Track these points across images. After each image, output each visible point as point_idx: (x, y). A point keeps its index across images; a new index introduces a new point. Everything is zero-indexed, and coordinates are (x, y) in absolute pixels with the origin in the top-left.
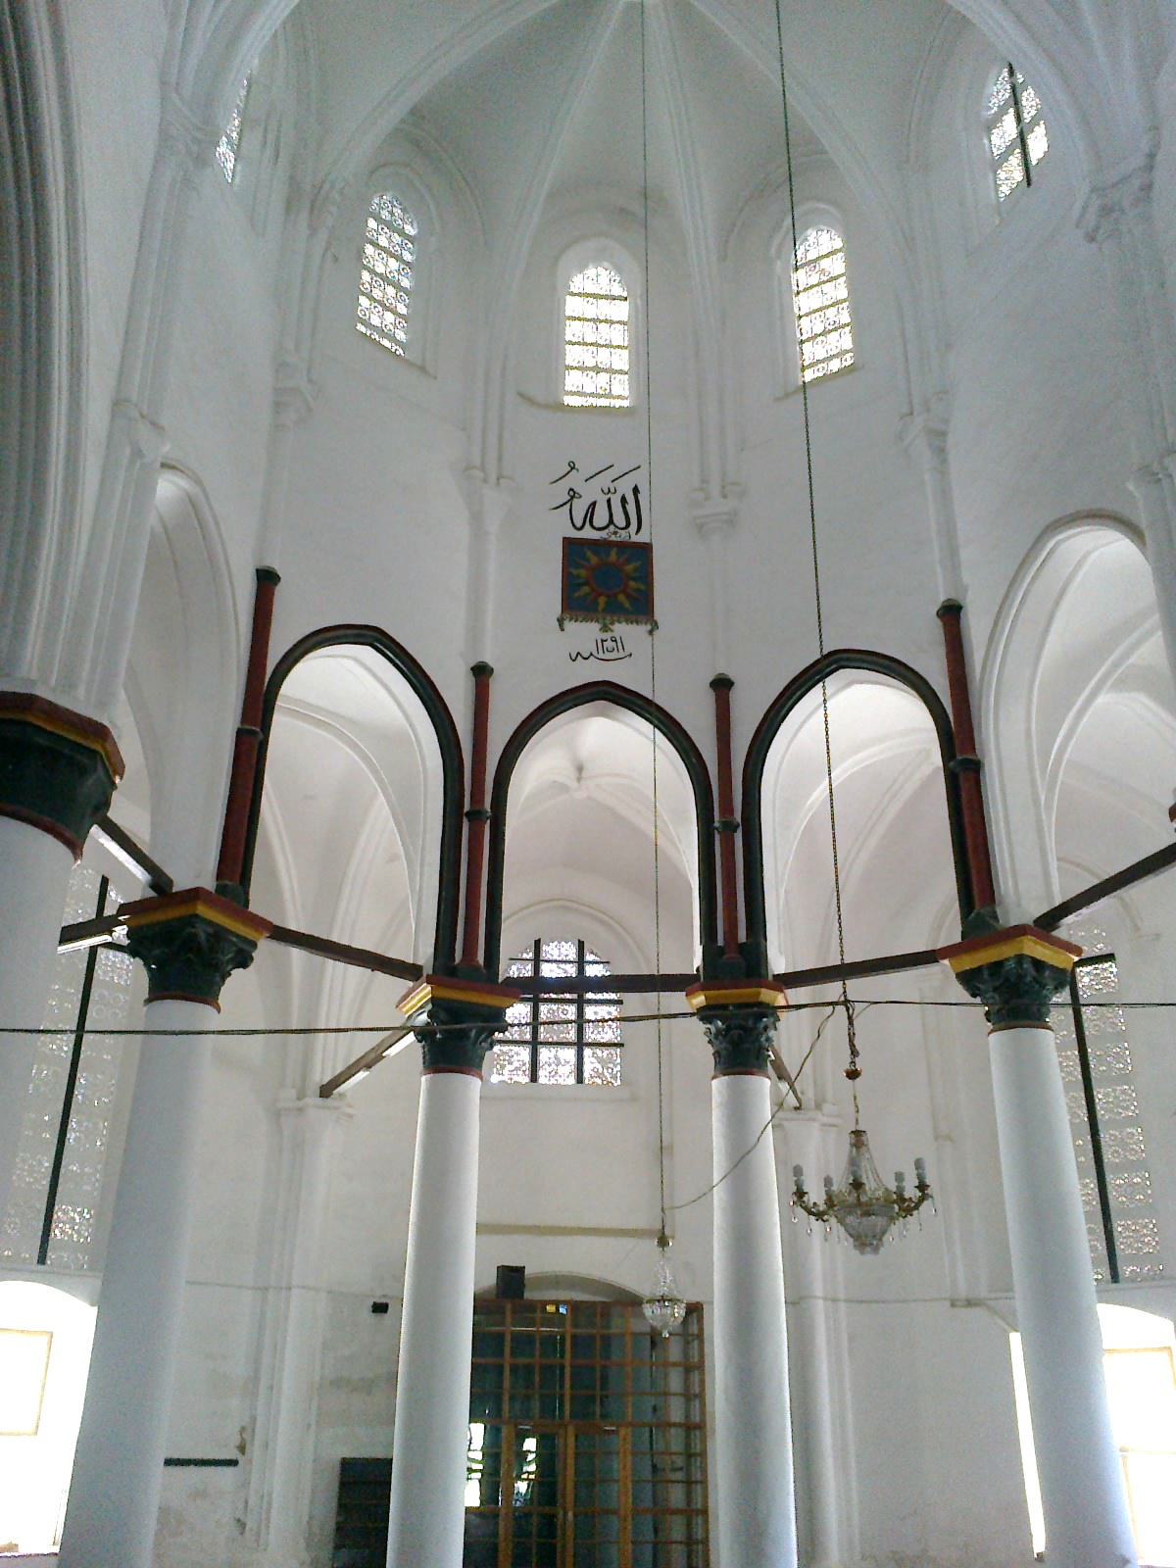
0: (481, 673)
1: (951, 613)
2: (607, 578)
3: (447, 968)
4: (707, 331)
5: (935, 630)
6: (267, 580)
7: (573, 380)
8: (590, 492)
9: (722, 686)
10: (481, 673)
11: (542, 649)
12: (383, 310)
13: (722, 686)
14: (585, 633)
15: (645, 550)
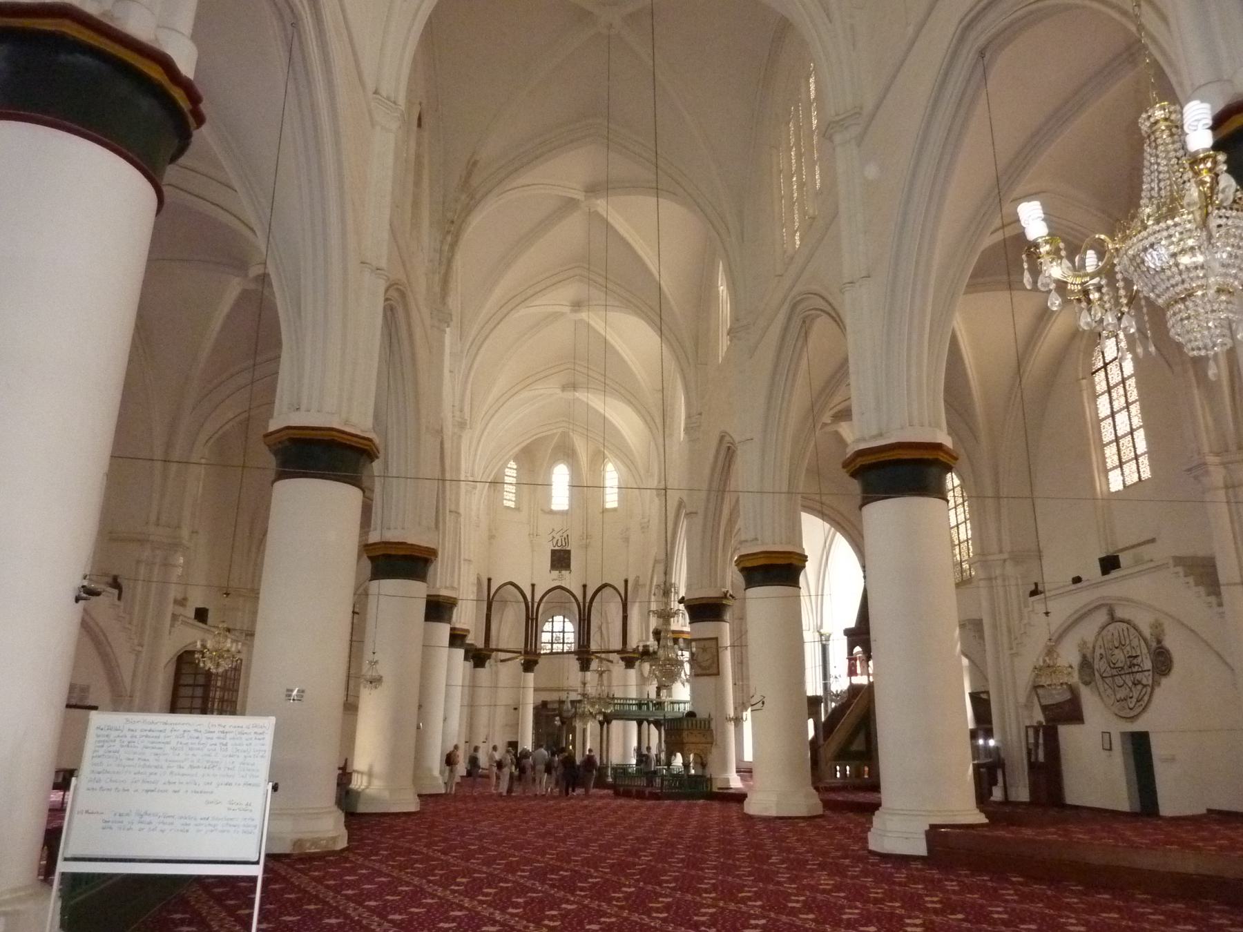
0: (533, 585)
1: (626, 581)
2: (561, 560)
3: (526, 653)
4: (585, 489)
5: (623, 583)
6: (489, 580)
7: (554, 500)
8: (557, 537)
9: (585, 586)
10: (533, 585)
11: (546, 578)
12: (509, 497)
13: (585, 586)
14: (556, 573)
15: (569, 552)
